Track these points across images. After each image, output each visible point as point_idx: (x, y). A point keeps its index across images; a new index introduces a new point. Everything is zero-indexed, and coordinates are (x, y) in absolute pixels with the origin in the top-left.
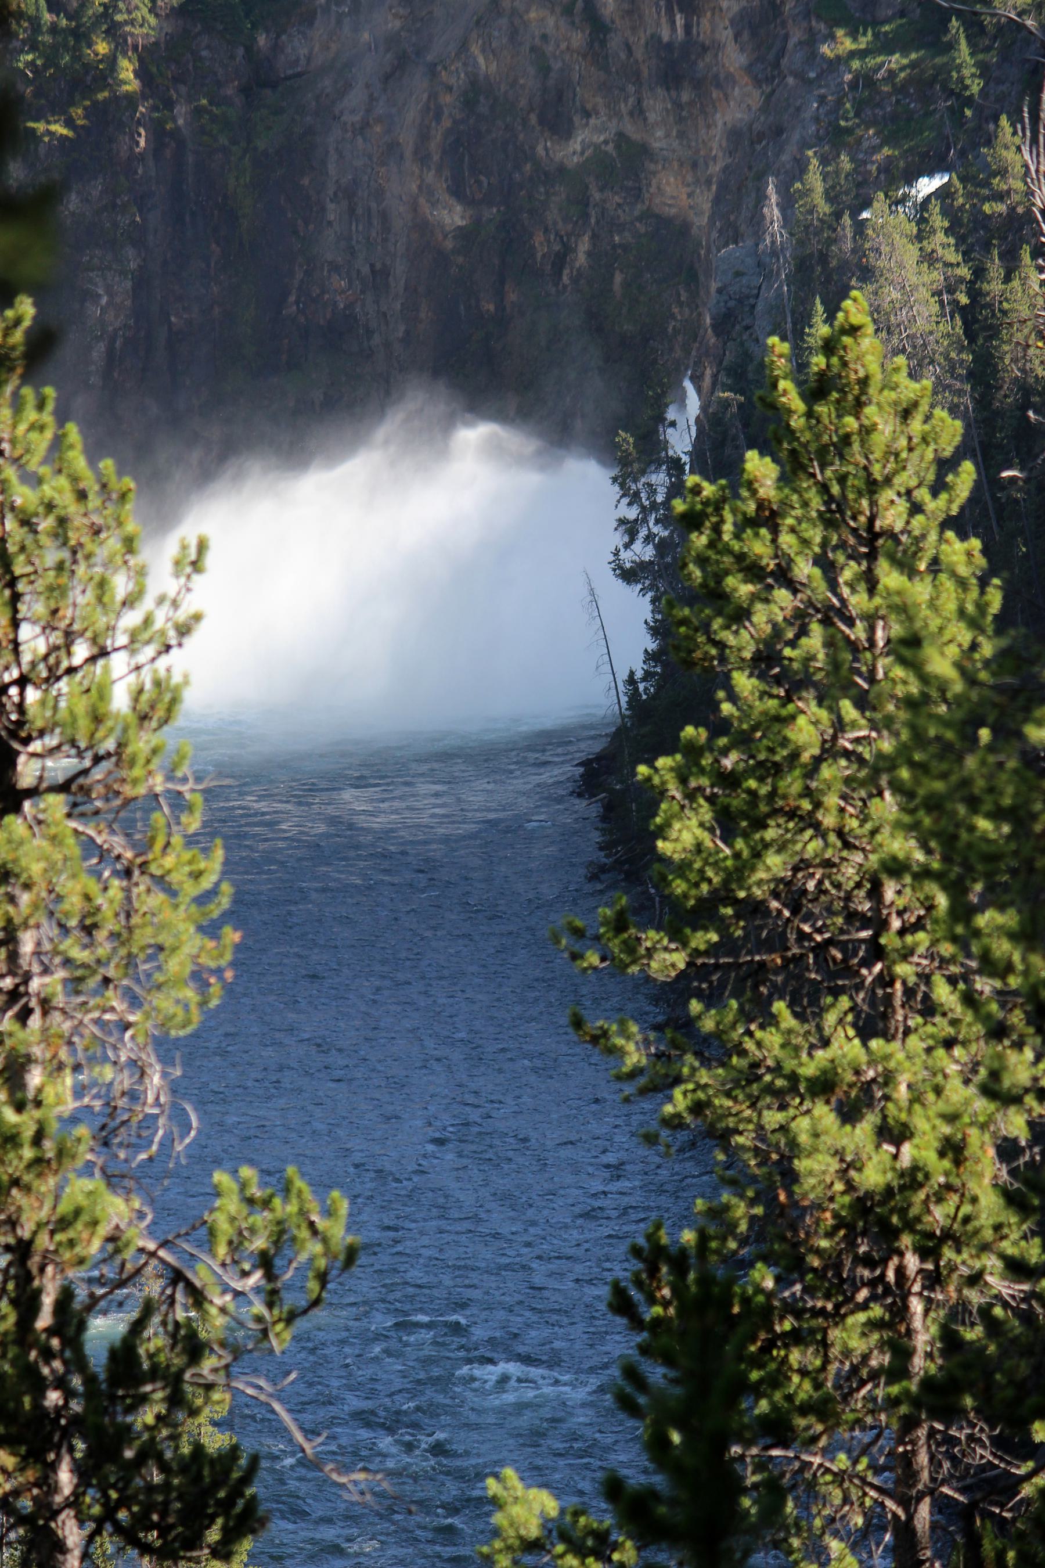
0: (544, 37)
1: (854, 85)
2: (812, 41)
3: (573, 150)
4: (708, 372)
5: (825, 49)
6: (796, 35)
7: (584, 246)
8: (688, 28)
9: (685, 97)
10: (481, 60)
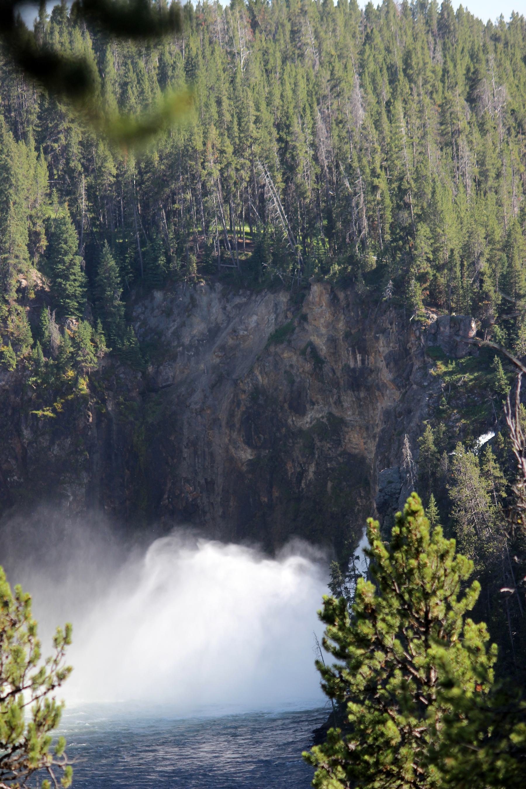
0: (291, 366)
3: (307, 421)
7: (312, 469)
9: (362, 395)
10: (260, 377)
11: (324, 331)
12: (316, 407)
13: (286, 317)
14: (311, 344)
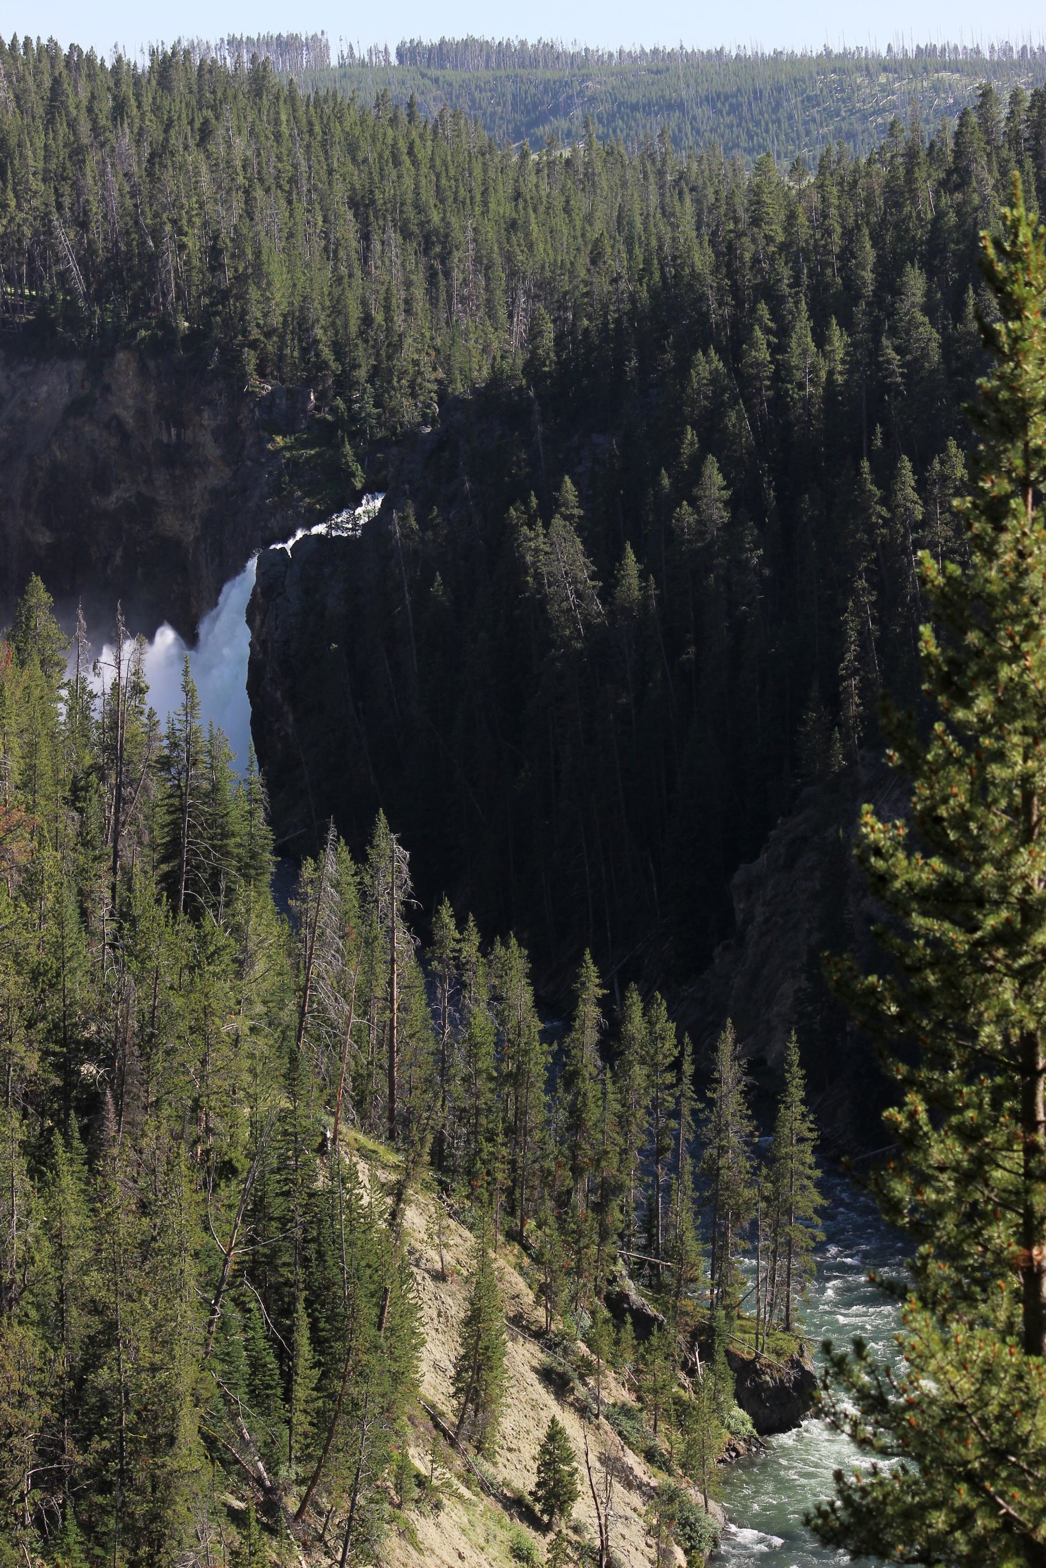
0: (93, 441)
1: (287, 465)
2: (261, 443)
4: (258, 618)
6: (250, 440)
7: (119, 553)
8: (178, 436)
9: (178, 472)
10: (58, 453)
11: (130, 402)
13: (83, 387)
14: (115, 417)
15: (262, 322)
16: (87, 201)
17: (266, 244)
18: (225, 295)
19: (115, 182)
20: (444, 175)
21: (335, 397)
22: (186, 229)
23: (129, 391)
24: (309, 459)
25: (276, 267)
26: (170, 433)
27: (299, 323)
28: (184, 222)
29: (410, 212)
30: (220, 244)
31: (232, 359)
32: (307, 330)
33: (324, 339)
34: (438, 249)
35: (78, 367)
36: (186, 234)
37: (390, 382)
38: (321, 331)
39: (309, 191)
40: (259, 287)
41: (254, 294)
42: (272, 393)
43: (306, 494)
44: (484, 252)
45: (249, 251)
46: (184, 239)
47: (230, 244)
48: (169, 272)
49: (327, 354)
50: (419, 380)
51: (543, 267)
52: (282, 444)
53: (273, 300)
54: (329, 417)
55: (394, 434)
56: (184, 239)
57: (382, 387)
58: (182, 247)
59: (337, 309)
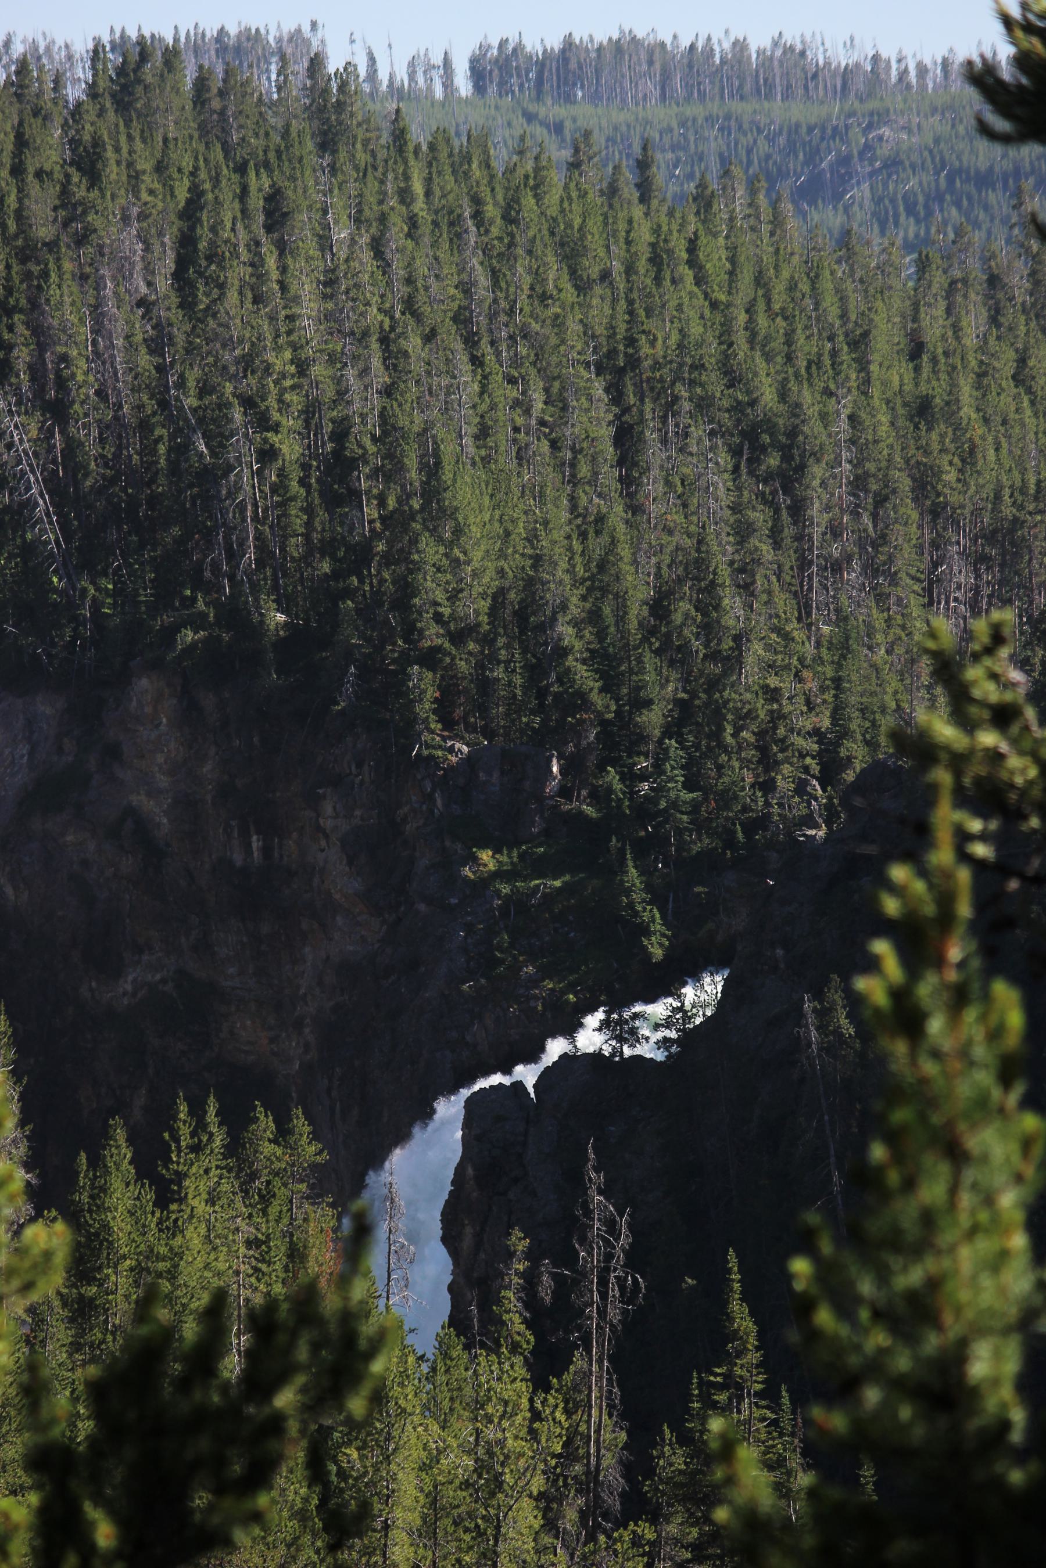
1: (504, 911)
3: (126, 988)
4: (468, 1230)
5: (467, 872)
8: (267, 851)
11: (163, 781)
12: (145, 957)
15: (446, 611)
16: (64, 358)
17: (448, 450)
18: (359, 557)
19: (122, 320)
20: (761, 306)
21: (601, 768)
22: (276, 416)
23: (160, 759)
24: (550, 898)
25: (466, 492)
26: (249, 845)
27: (522, 613)
28: (272, 402)
29: (714, 383)
30: (352, 448)
31: (386, 689)
32: (541, 628)
33: (578, 645)
34: (773, 461)
35: (47, 708)
36: (276, 428)
37: (717, 735)
38: (570, 630)
39: (511, 337)
40: (440, 540)
41: (430, 551)
42: (469, 761)
43: (546, 972)
44: (871, 466)
45: (412, 462)
46: (274, 438)
47: (371, 448)
48: (242, 508)
49: (585, 677)
50: (781, 732)
51: (998, 497)
52: (492, 866)
53: (467, 567)
54: (589, 810)
55: (730, 842)
56: (274, 438)
57: (697, 746)
58: (268, 454)
59: (600, 581)
